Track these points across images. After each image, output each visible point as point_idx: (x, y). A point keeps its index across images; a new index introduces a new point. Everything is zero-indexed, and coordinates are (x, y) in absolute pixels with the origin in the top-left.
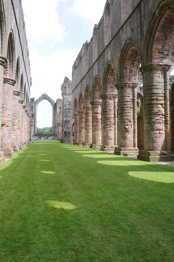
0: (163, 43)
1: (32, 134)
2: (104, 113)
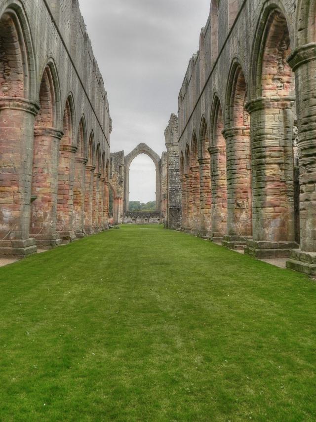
0: (279, 64)
1: (119, 213)
2: (213, 179)
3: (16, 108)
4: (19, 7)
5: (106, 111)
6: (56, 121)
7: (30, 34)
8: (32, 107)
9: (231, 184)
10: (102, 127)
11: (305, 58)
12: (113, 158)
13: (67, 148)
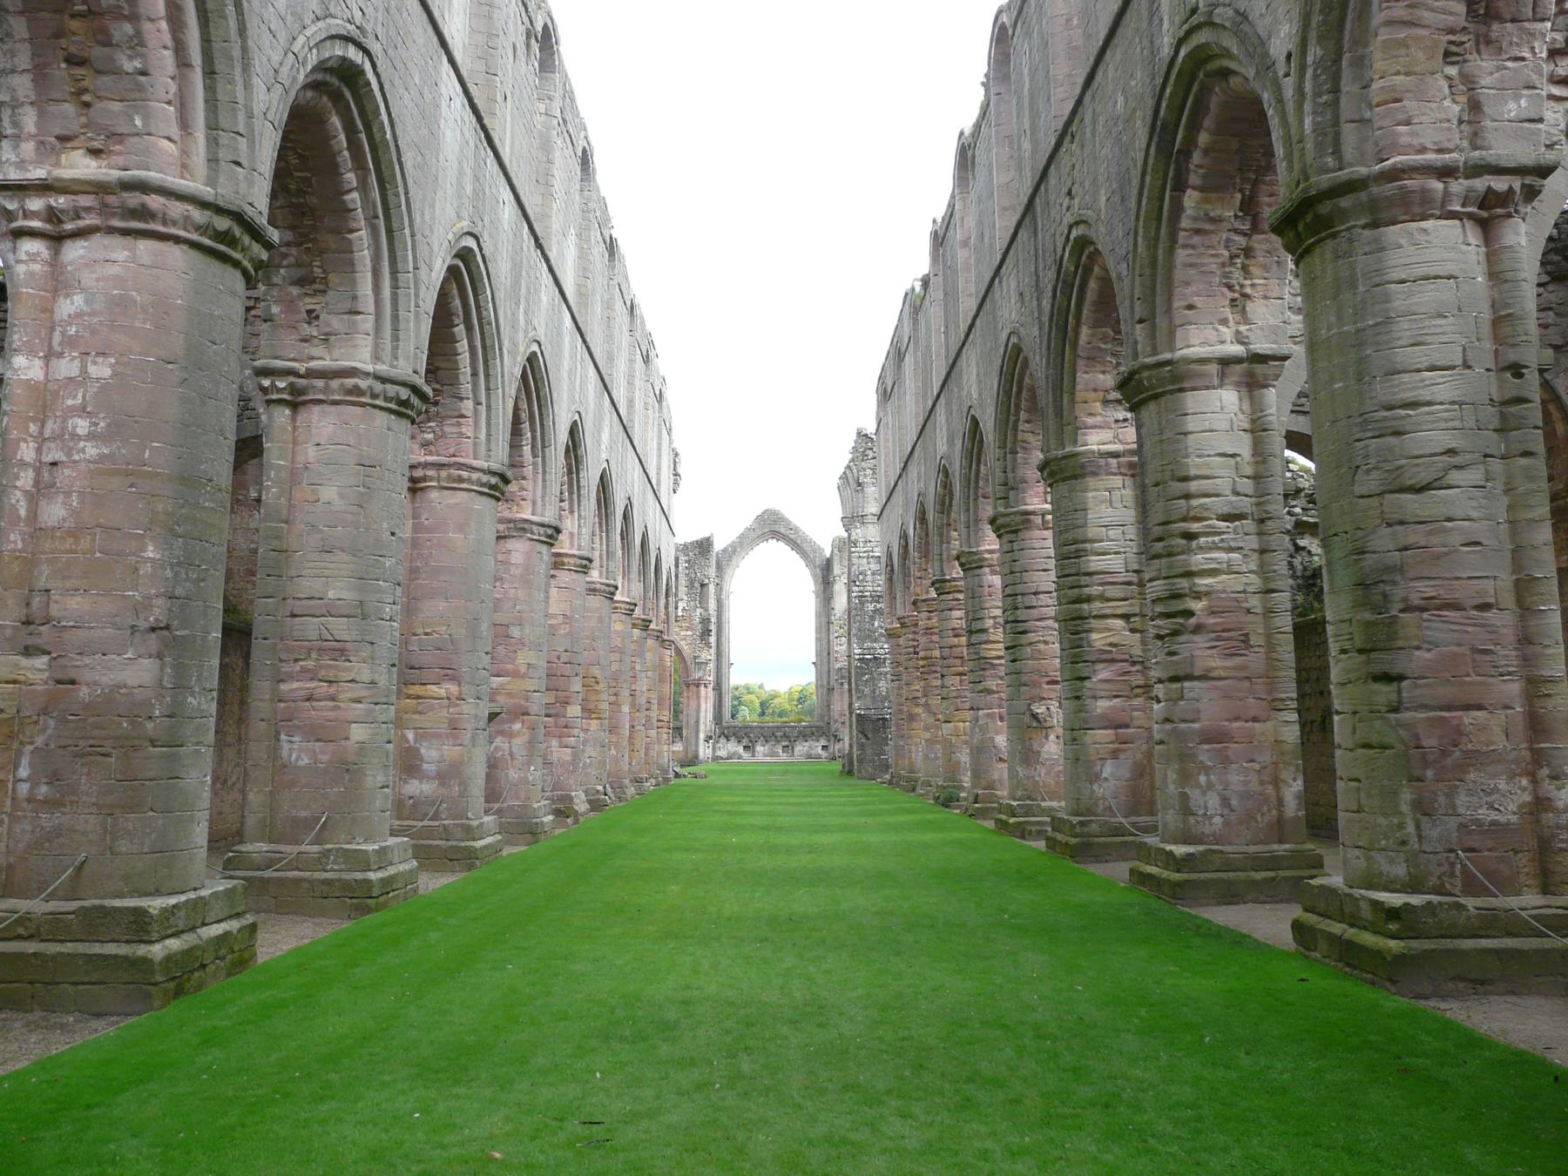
1: (702, 727)
4: (471, 250)
5: (665, 432)
6: (543, 497)
8: (494, 480)
9: (1014, 661)
10: (654, 482)
11: (1152, 387)
12: (682, 558)
13: (566, 560)
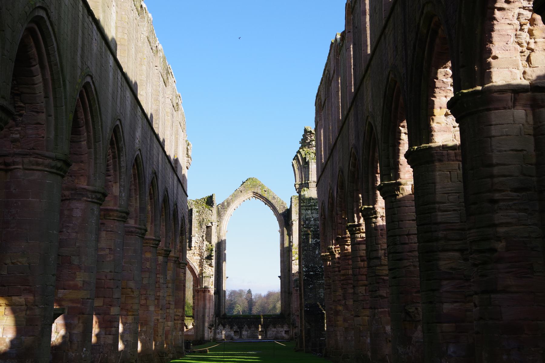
1: (207, 319)
3: (34, 167)
4: (42, 18)
7: (56, 53)
8: (59, 164)
13: (111, 214)
